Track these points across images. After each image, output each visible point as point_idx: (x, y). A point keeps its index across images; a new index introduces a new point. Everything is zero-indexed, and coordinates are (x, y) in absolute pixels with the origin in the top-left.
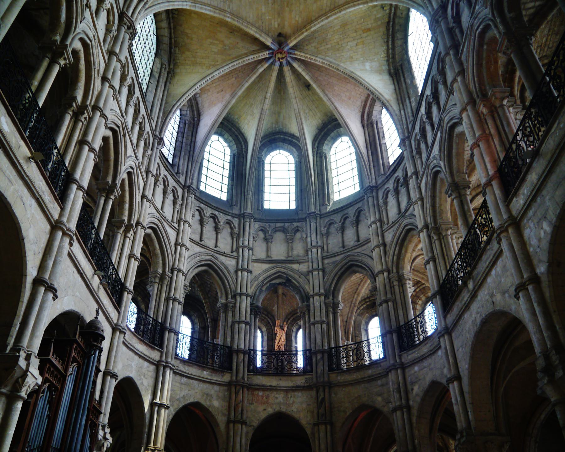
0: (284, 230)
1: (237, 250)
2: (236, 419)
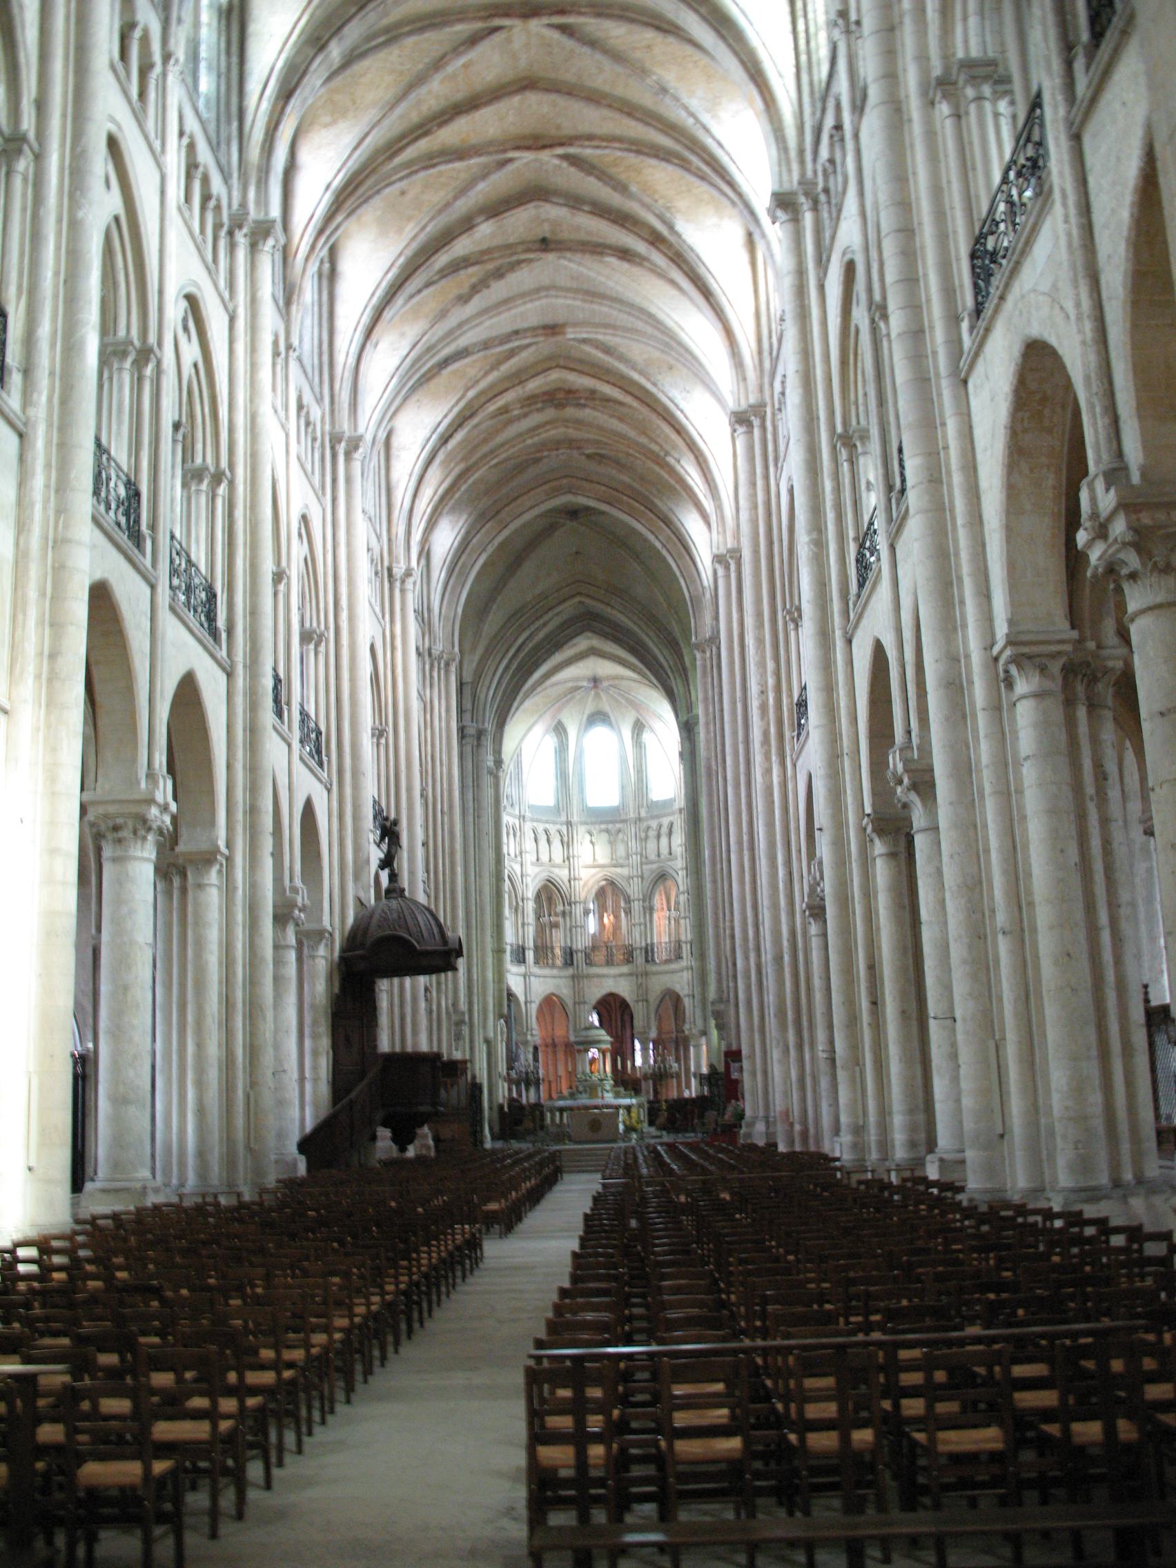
0: (607, 831)
1: (568, 858)
2: (579, 1002)
